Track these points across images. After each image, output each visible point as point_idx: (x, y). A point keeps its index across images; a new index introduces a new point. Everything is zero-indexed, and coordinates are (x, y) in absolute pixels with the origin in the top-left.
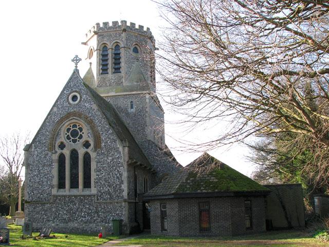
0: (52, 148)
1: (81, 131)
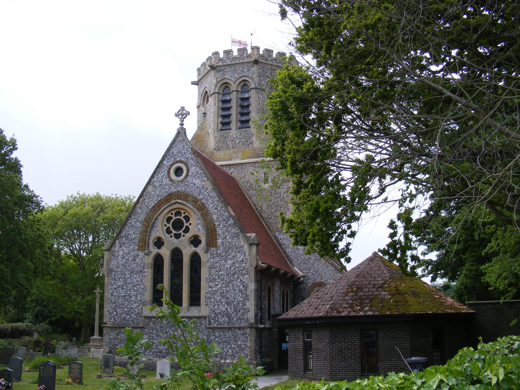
0: (143, 245)
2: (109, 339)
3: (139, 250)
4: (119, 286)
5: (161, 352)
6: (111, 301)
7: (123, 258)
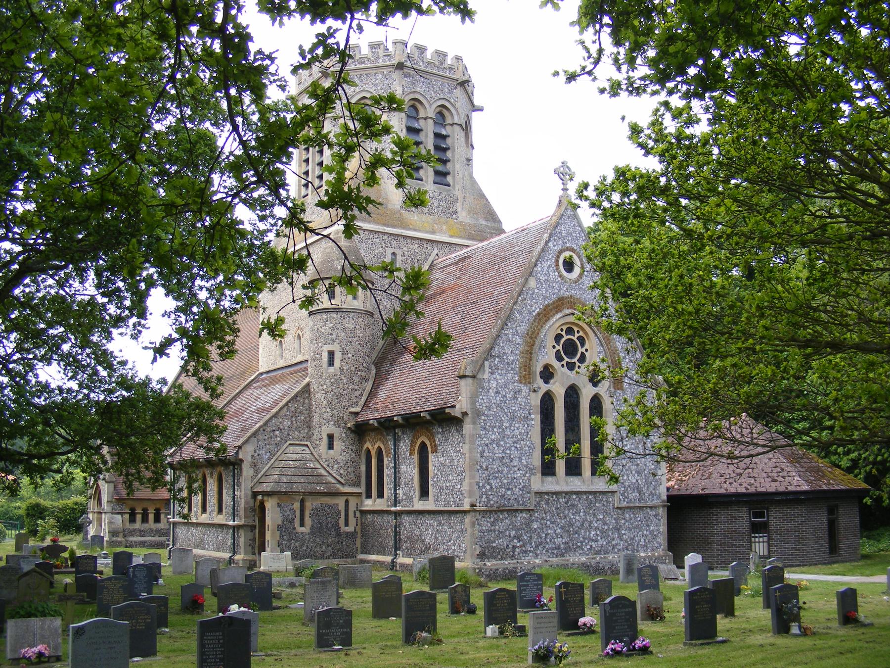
0: (526, 376)
1: (583, 345)
2: (480, 531)
3: (521, 383)
4: (493, 441)
5: (558, 548)
6: (481, 467)
7: (497, 393)
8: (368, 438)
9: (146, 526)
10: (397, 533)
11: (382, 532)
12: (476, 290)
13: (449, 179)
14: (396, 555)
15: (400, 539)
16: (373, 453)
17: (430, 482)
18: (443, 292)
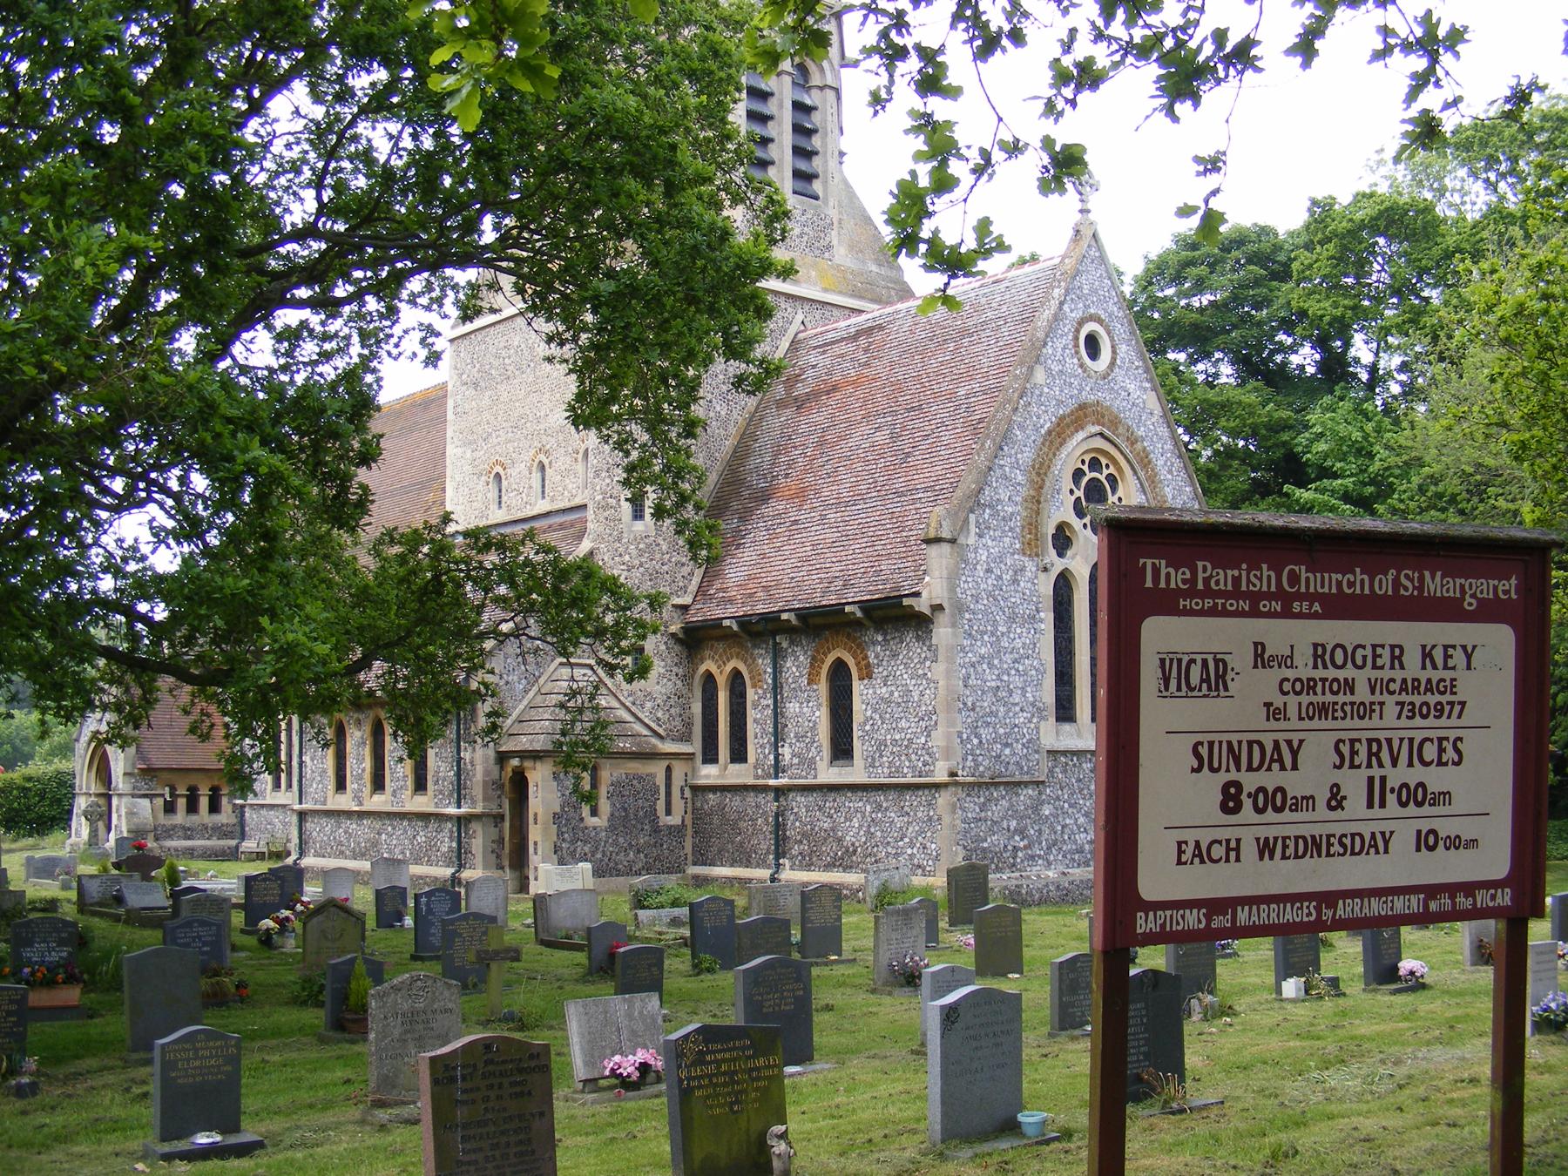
0: (1031, 547)
1: (1114, 490)
2: (964, 821)
4: (983, 657)
8: (707, 653)
9: (194, 818)
10: (779, 826)
11: (742, 824)
12: (914, 387)
13: (817, 186)
14: (778, 866)
15: (785, 838)
16: (722, 681)
17: (856, 733)
18: (835, 389)
